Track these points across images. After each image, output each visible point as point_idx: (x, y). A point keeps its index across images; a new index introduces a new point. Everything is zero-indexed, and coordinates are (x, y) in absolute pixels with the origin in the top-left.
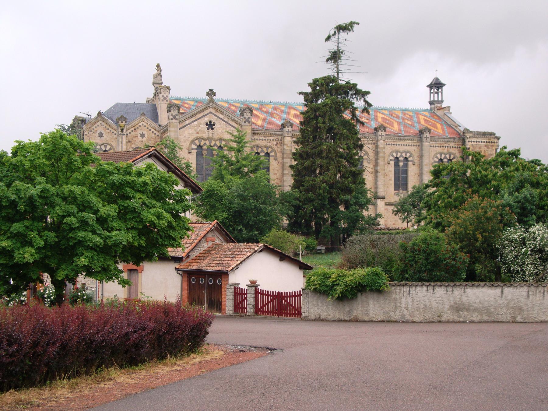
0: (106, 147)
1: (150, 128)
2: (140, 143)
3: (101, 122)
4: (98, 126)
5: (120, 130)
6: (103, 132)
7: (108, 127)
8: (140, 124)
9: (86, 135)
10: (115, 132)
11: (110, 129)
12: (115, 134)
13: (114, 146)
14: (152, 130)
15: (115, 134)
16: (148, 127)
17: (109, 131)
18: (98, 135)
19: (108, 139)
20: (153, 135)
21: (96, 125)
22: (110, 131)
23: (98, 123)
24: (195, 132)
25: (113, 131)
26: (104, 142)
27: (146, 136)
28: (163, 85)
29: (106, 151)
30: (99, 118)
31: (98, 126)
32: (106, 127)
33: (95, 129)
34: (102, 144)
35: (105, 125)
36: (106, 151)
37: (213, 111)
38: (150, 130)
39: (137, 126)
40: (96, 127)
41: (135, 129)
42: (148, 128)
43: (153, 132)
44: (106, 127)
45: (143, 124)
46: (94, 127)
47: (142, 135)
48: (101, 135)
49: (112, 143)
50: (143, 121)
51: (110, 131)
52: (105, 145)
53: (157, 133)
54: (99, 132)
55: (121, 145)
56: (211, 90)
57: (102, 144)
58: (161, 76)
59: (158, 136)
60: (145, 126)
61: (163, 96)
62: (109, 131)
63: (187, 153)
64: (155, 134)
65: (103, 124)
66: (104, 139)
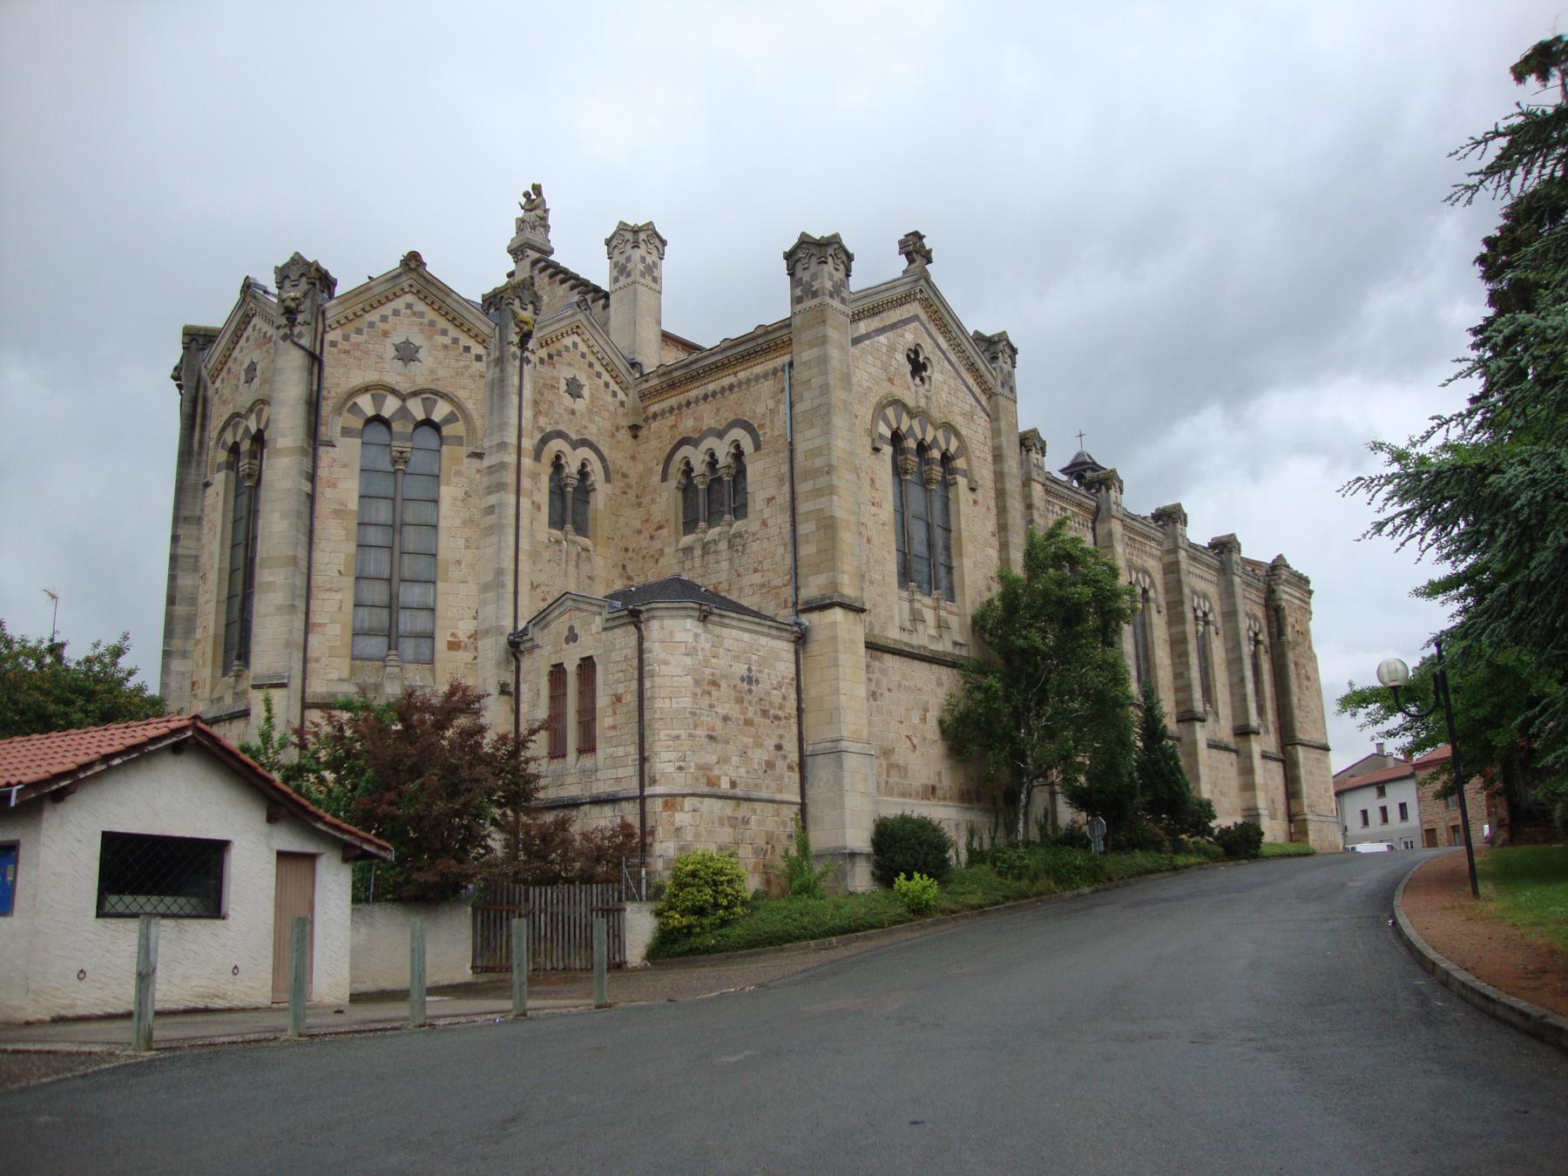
0: (429, 406)
1: (598, 367)
2: (566, 417)
3: (409, 298)
4: (396, 313)
5: (516, 339)
6: (417, 340)
7: (442, 323)
8: (568, 341)
9: (333, 344)
10: (477, 349)
11: (453, 332)
12: (478, 358)
13: (470, 405)
14: (606, 377)
15: (478, 358)
16: (593, 359)
17: (447, 340)
18: (392, 352)
19: (441, 373)
20: (609, 399)
21: (387, 310)
22: (455, 341)
23: (399, 304)
24: (884, 376)
25: (465, 340)
26: (422, 382)
27: (586, 392)
28: (552, 258)
29: (428, 422)
30: (405, 282)
31: (396, 313)
32: (432, 324)
33: (354, 338)
34: (415, 394)
35: (431, 315)
36: (428, 422)
37: (924, 317)
38: (599, 375)
39: (558, 345)
40: (384, 319)
41: (550, 356)
42: (591, 365)
43: (607, 385)
44: (432, 324)
45: (575, 345)
46: (374, 316)
47: (574, 389)
48: (407, 354)
49: (461, 394)
50: (576, 331)
51: (455, 341)
52: (430, 395)
53: (621, 396)
54: (398, 338)
55: (515, 399)
56: (917, 236)
57: (415, 394)
58: (547, 228)
59: (622, 404)
60: (583, 355)
61: (643, 259)
62: (441, 340)
63: (869, 449)
64: (614, 394)
65: (420, 306)
66: (420, 374)
